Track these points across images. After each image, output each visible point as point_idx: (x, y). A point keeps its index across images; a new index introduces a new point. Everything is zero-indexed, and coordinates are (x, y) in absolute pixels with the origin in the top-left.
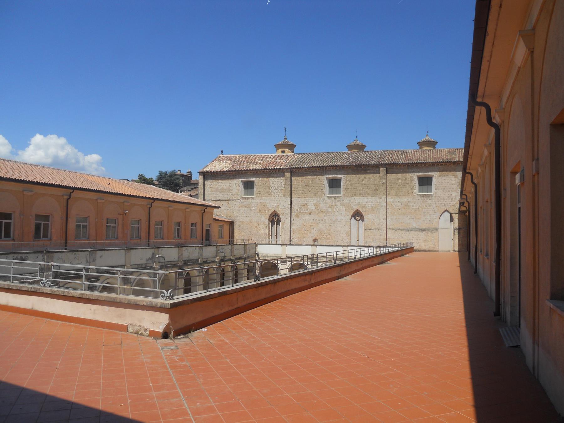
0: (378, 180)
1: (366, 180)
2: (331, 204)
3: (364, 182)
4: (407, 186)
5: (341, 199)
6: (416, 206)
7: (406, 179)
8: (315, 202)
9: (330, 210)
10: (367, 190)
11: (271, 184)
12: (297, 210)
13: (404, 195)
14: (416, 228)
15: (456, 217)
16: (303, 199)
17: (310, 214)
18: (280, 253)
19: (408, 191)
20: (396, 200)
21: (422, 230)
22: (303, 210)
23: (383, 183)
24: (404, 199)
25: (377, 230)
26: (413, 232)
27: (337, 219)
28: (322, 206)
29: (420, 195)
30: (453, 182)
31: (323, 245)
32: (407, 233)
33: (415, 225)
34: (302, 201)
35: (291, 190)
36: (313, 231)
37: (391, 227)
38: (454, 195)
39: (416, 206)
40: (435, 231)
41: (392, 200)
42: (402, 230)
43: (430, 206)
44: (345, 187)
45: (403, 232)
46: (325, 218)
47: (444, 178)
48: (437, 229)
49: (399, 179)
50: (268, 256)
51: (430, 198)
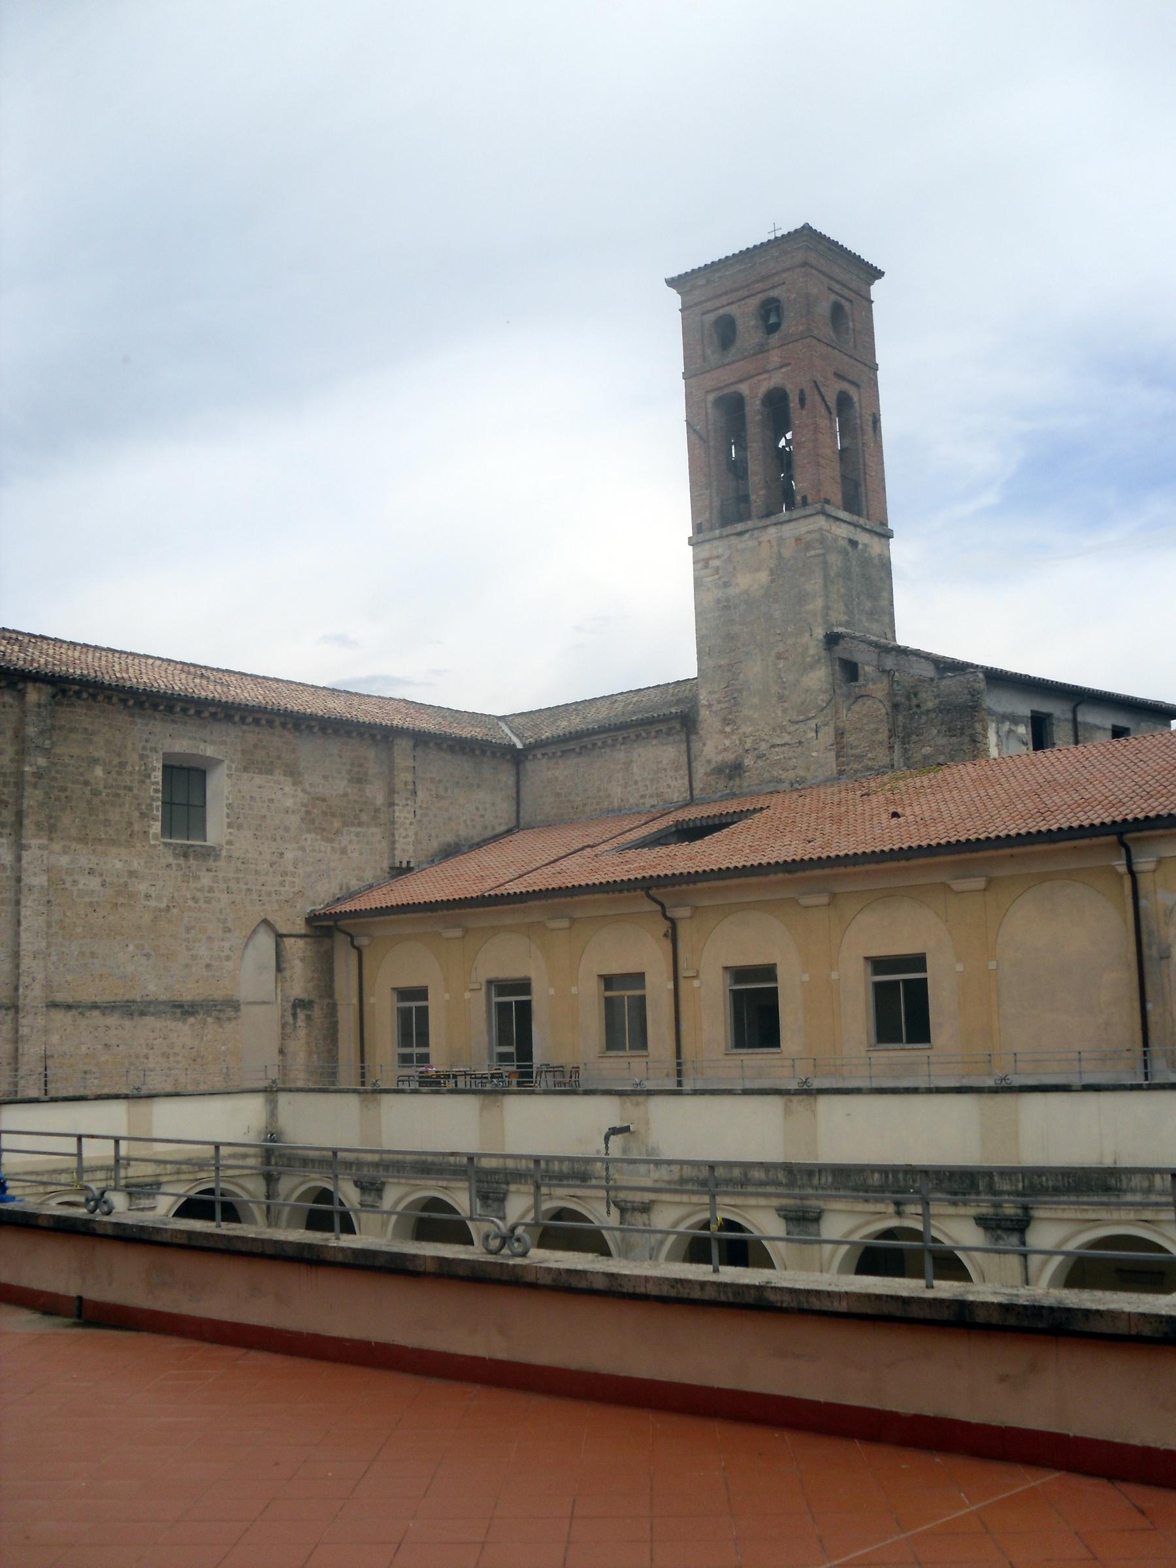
6: (159, 898)
7: (122, 764)
13: (113, 842)
14: (157, 1003)
15: (296, 948)
19: (130, 823)
20: (83, 861)
21: (184, 1010)
23: (39, 775)
24: (115, 862)
26: (148, 1020)
29: (175, 847)
30: (289, 803)
32: (127, 1023)
33: (154, 988)
38: (289, 856)
39: (159, 898)
40: (230, 1013)
42: (107, 1008)
43: (208, 901)
45: (113, 1020)
47: (258, 779)
48: (235, 1005)
49: (96, 761)
51: (211, 863)
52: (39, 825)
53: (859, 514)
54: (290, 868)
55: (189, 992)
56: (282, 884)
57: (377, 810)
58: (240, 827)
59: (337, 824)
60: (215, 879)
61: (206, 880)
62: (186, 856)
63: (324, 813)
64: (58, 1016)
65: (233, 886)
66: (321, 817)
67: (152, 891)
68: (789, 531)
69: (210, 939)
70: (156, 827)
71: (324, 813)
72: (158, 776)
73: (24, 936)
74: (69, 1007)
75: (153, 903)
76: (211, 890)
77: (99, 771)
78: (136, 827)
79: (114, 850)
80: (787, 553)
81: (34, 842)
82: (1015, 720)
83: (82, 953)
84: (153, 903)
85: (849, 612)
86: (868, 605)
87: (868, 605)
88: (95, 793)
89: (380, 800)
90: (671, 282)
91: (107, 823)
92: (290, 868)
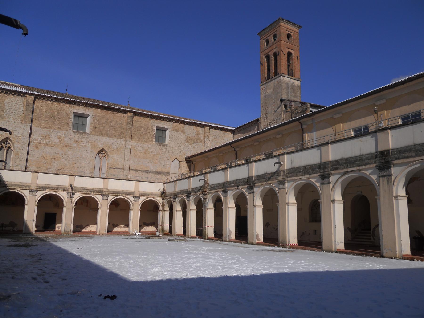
0: (125, 124)
1: (114, 122)
2: (77, 139)
3: (111, 124)
5: (88, 136)
6: (154, 152)
7: (148, 128)
8: (60, 134)
9: (75, 145)
10: (113, 132)
11: (6, 107)
12: (37, 140)
13: (145, 142)
14: (153, 171)
16: (46, 130)
17: (52, 146)
18: (30, 181)
19: (149, 139)
21: (158, 173)
22: (44, 141)
24: (145, 145)
25: (120, 170)
27: (82, 156)
28: (67, 140)
30: (182, 137)
31: (83, 176)
32: (146, 174)
33: (152, 168)
34: (44, 131)
35: (32, 118)
36: (55, 164)
37: (133, 168)
38: (182, 147)
41: (135, 144)
42: (142, 171)
44: (93, 125)
45: (144, 173)
46: (69, 153)
47: (176, 133)
48: (169, 173)
49: (142, 127)
50: (12, 186)
52: (129, 137)
53: (292, 76)
54: (182, 149)
55: (160, 170)
56: (180, 152)
57: (201, 140)
58: (172, 141)
59: (192, 142)
60: (166, 150)
61: (164, 150)
62: (160, 145)
63: (190, 140)
64: (131, 171)
65: (170, 152)
66: (189, 140)
67: (153, 151)
68: (276, 80)
69: (164, 161)
70: (154, 140)
71: (190, 140)
72: (155, 130)
73: (126, 156)
74: (135, 170)
75: (153, 153)
76: (165, 152)
77: (143, 129)
78: (150, 139)
80: (275, 85)
83: (138, 161)
84: (153, 153)
87: (294, 94)
88: (142, 133)
89: (202, 138)
90: (258, 34)
92: (182, 149)
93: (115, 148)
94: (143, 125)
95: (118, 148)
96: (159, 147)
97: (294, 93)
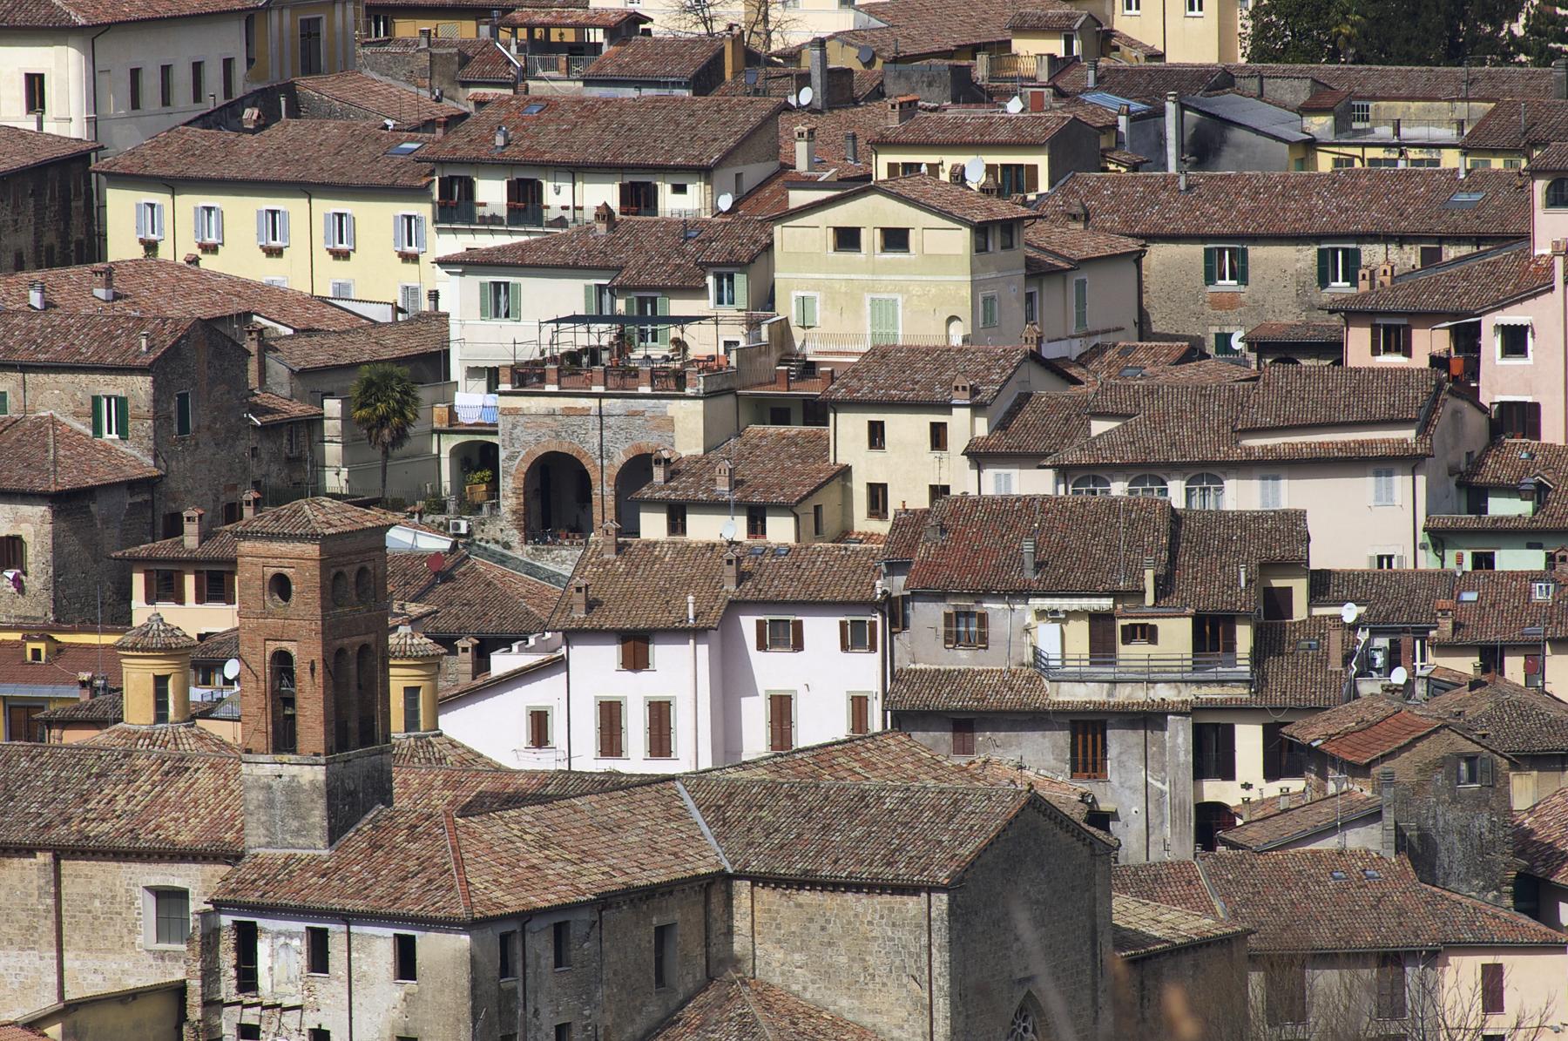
4: (118, 919)
7: (114, 897)
13: (109, 951)
20: (90, 964)
41: (77, 964)
53: (294, 752)
62: (162, 959)
77: (97, 903)
79: (110, 957)
81: (47, 955)
82: (290, 935)
85: (270, 833)
86: (295, 824)
87: (295, 824)
88: (96, 918)
91: (105, 938)
93: (16, 986)
94: (95, 888)
95: (23, 986)
96: (158, 967)
97: (295, 817)
